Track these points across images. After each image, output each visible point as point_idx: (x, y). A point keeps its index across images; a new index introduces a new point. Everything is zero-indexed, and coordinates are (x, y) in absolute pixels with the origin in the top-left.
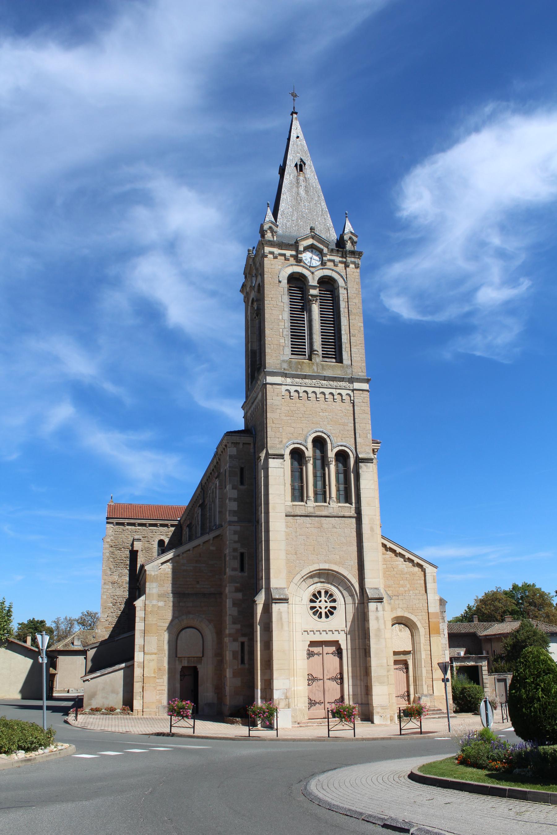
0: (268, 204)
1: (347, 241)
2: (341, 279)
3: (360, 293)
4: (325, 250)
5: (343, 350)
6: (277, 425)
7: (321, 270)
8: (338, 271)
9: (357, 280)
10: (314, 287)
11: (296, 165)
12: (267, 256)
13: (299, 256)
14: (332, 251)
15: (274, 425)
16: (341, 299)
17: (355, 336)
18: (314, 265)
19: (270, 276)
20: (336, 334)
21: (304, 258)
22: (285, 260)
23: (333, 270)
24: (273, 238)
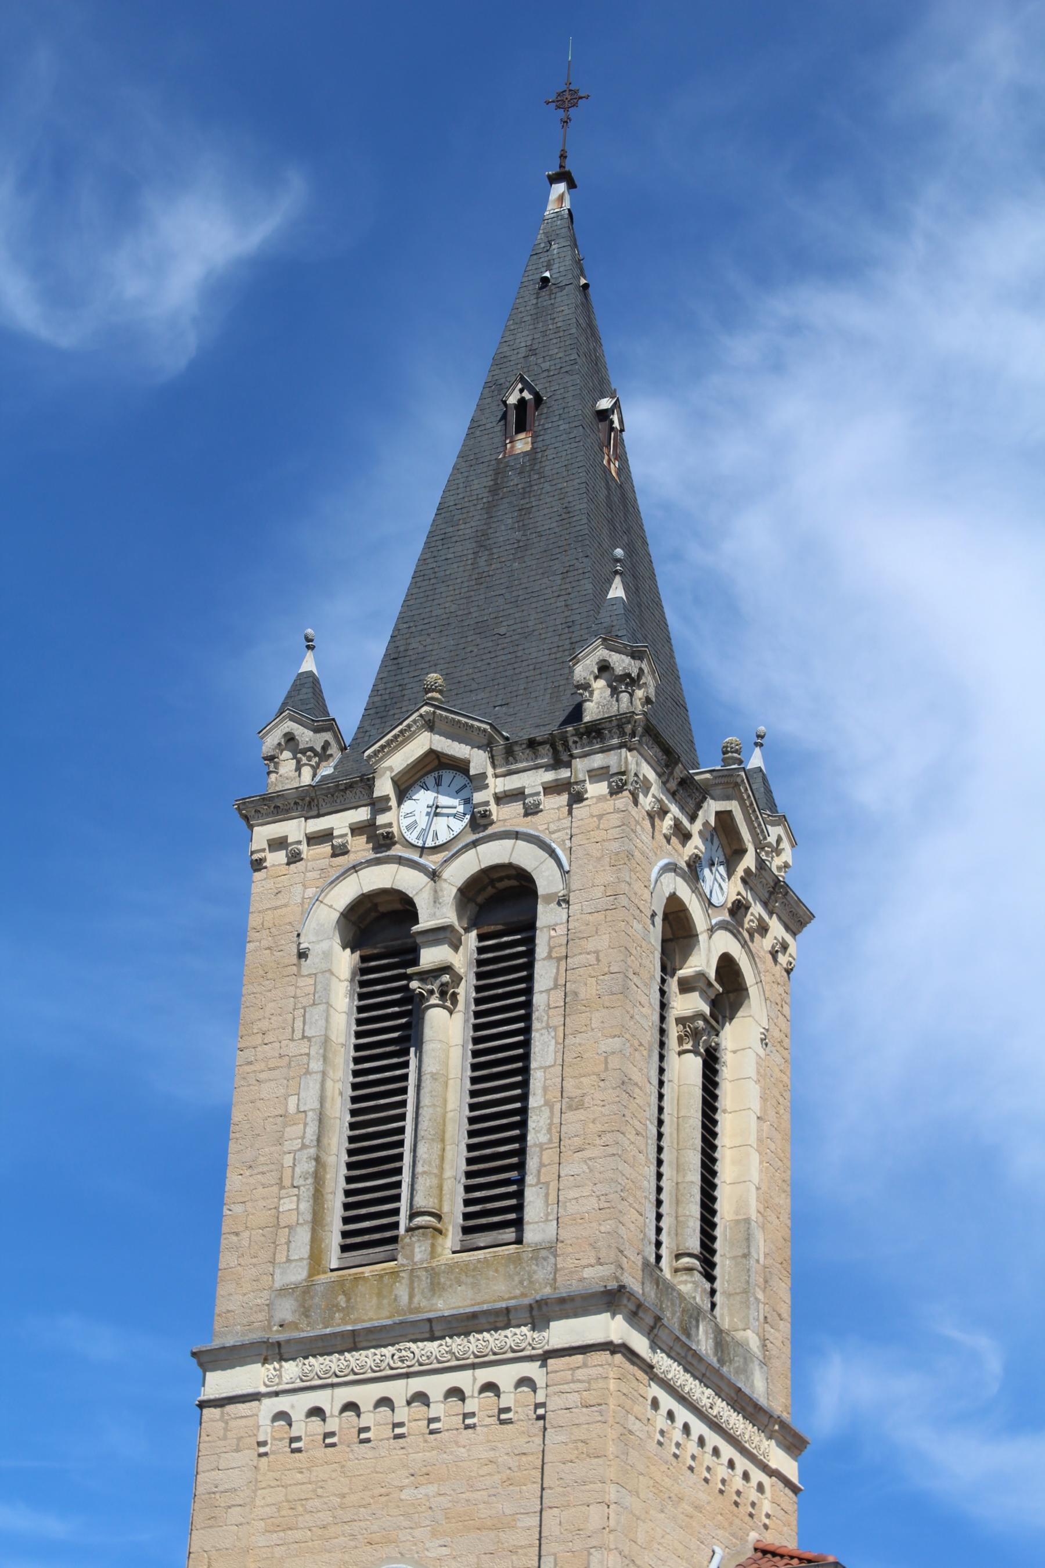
2: (552, 862)
4: (478, 760)
7: (472, 851)
10: (441, 934)
18: (444, 837)
23: (517, 835)
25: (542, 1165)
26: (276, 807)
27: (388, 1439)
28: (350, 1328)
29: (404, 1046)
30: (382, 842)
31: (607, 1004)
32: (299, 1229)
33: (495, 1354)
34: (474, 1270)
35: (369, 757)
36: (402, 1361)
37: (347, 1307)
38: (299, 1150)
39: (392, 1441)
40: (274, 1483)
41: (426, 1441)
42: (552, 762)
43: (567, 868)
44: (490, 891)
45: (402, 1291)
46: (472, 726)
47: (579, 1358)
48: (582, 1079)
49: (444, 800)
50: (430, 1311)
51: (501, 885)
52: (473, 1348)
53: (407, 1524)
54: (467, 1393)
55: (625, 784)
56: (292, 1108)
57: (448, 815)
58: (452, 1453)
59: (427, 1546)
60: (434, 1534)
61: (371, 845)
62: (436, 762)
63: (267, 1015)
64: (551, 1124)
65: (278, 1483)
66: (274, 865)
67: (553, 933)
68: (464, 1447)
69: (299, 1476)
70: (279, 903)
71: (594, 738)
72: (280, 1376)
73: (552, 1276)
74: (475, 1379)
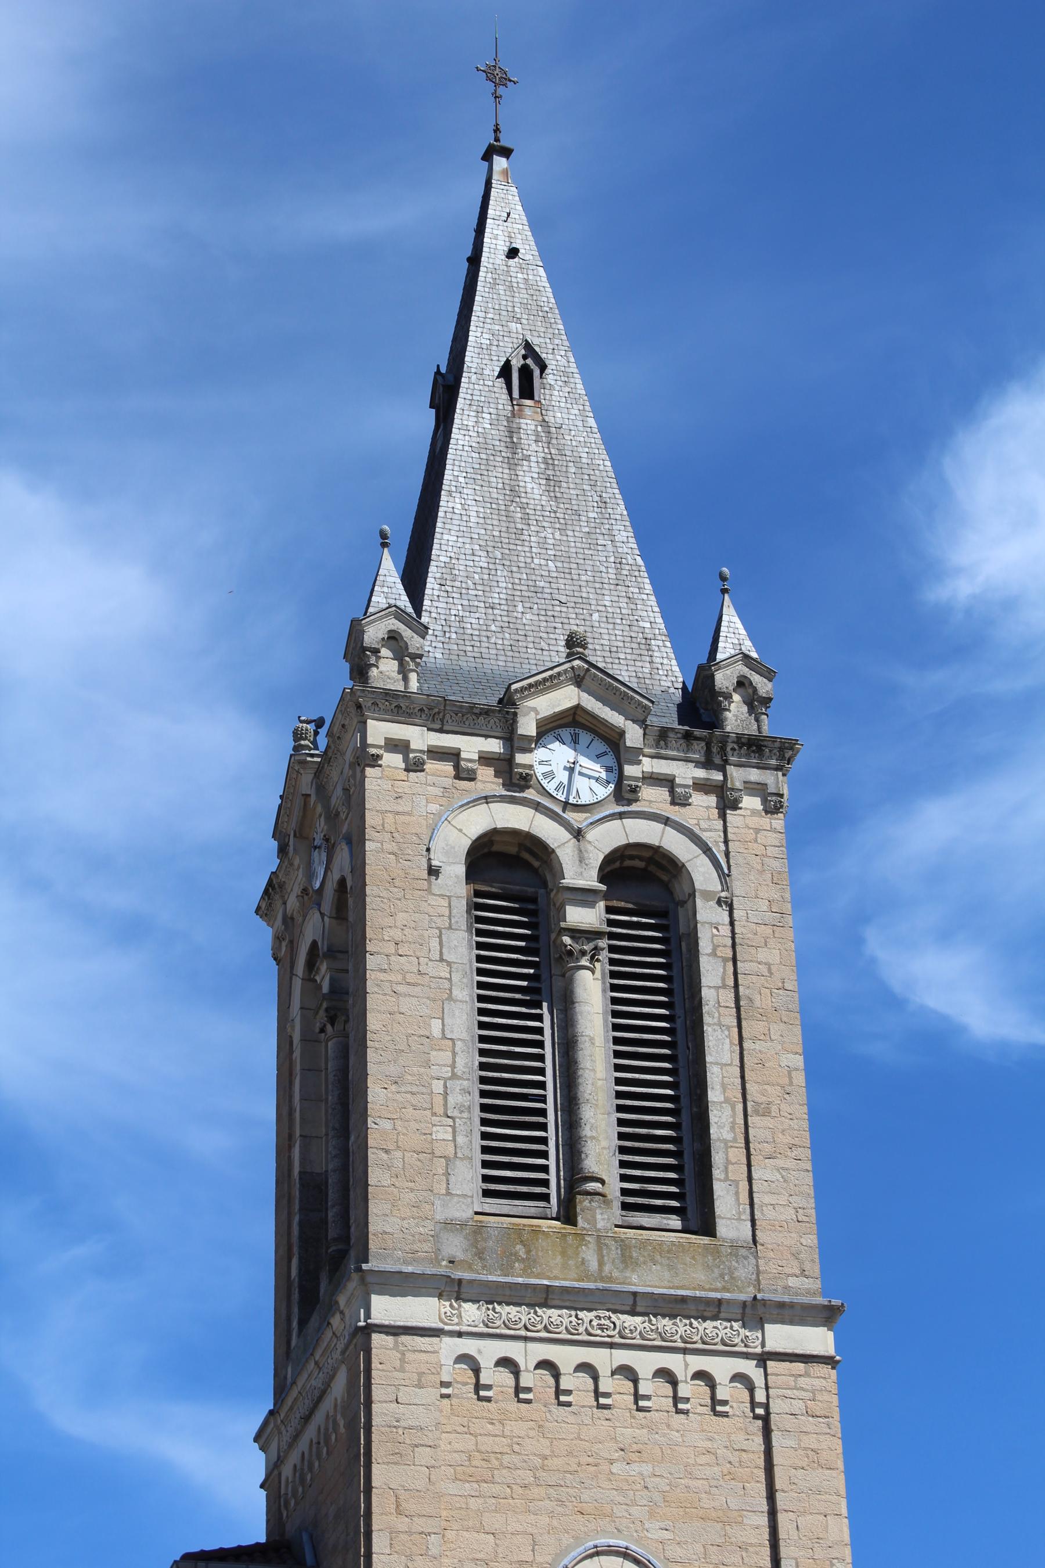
0: (383, 535)
1: (728, 697)
3: (789, 920)
4: (634, 735)
5: (717, 1173)
6: (419, 1524)
7: (617, 823)
8: (690, 823)
9: (776, 864)
11: (505, 372)
12: (379, 757)
13: (520, 758)
14: (663, 735)
15: (402, 1523)
16: (705, 945)
17: (766, 1113)
18: (586, 798)
19: (390, 846)
20: (684, 1101)
21: (539, 770)
22: (457, 777)
23: (667, 821)
24: (406, 679)
25: (728, 1162)
26: (398, 707)
27: (590, 1407)
28: (546, 1282)
29: (536, 997)
30: (515, 781)
31: (784, 1019)
32: (458, 1162)
33: (704, 1343)
34: (668, 1252)
35: (516, 690)
36: (602, 1330)
37: (528, 1259)
38: (450, 1079)
39: (595, 1410)
40: (460, 1429)
41: (634, 1418)
42: (703, 759)
43: (726, 871)
44: (617, 864)
45: (590, 1255)
46: (632, 698)
47: (800, 1367)
48: (766, 1087)
49: (584, 761)
50: (624, 1283)
51: (628, 863)
52: (681, 1330)
53: (621, 1499)
54: (680, 1376)
55: (782, 807)
56: (436, 1032)
57: (590, 777)
58: (664, 1435)
59: (646, 1526)
60: (652, 1515)
61: (501, 781)
62: (570, 718)
63: (399, 924)
64: (734, 1123)
65: (466, 1429)
66: (389, 766)
67: (715, 931)
68: (678, 1431)
69: (489, 1426)
70: (401, 809)
71: (753, 751)
72: (460, 1316)
73: (754, 1277)
74: (687, 1365)
